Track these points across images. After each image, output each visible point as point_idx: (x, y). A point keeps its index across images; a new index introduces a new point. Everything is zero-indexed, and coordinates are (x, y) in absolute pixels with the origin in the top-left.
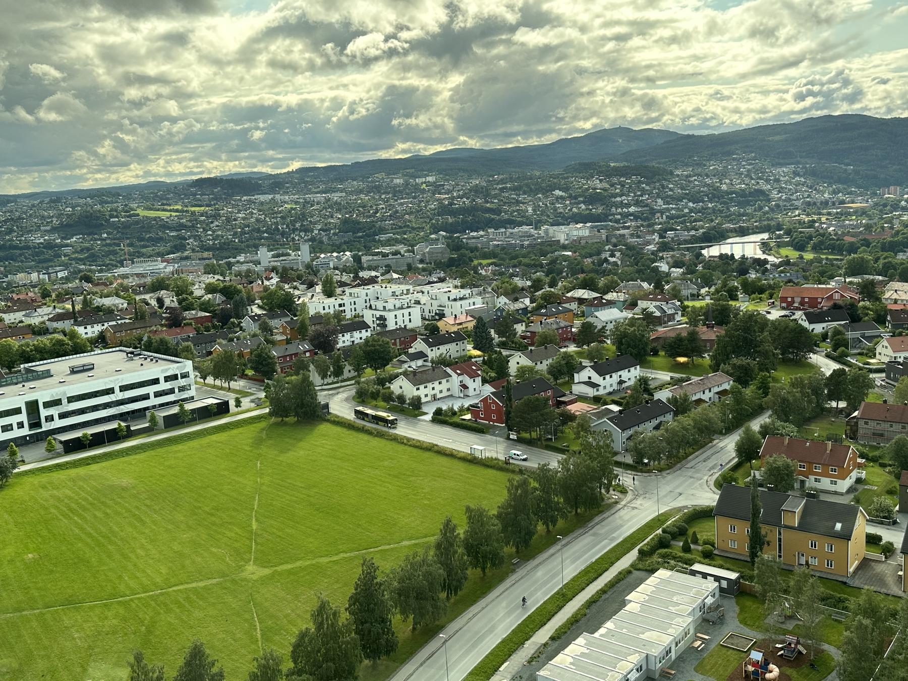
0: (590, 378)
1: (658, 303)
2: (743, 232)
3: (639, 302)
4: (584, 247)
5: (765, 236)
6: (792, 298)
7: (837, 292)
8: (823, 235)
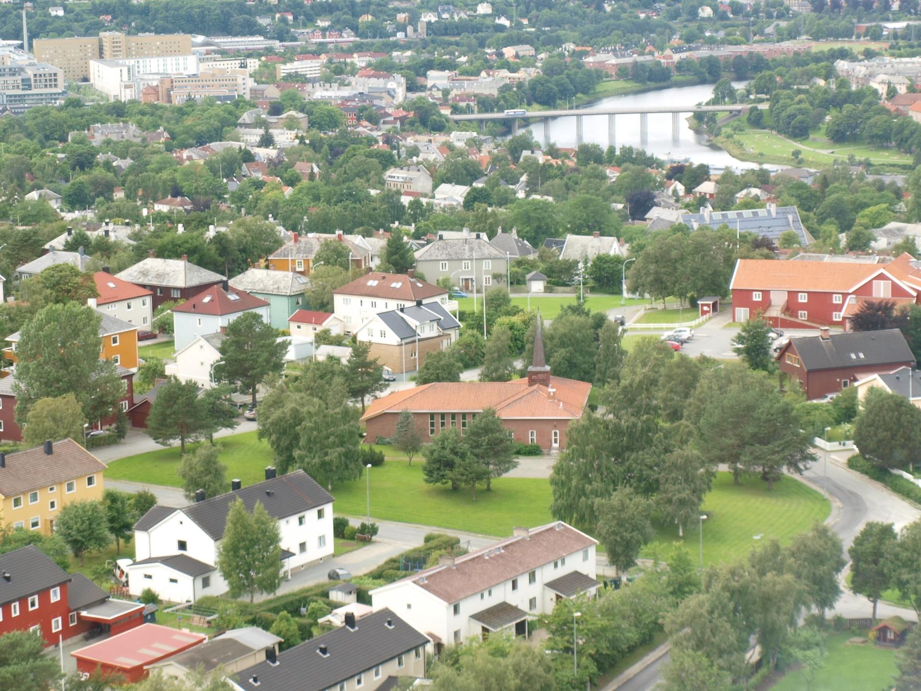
0: (182, 545)
1: (393, 305)
2: (653, 79)
3: (338, 300)
4: (181, 112)
5: (703, 95)
6: (766, 293)
7: (881, 277)
8: (857, 97)
